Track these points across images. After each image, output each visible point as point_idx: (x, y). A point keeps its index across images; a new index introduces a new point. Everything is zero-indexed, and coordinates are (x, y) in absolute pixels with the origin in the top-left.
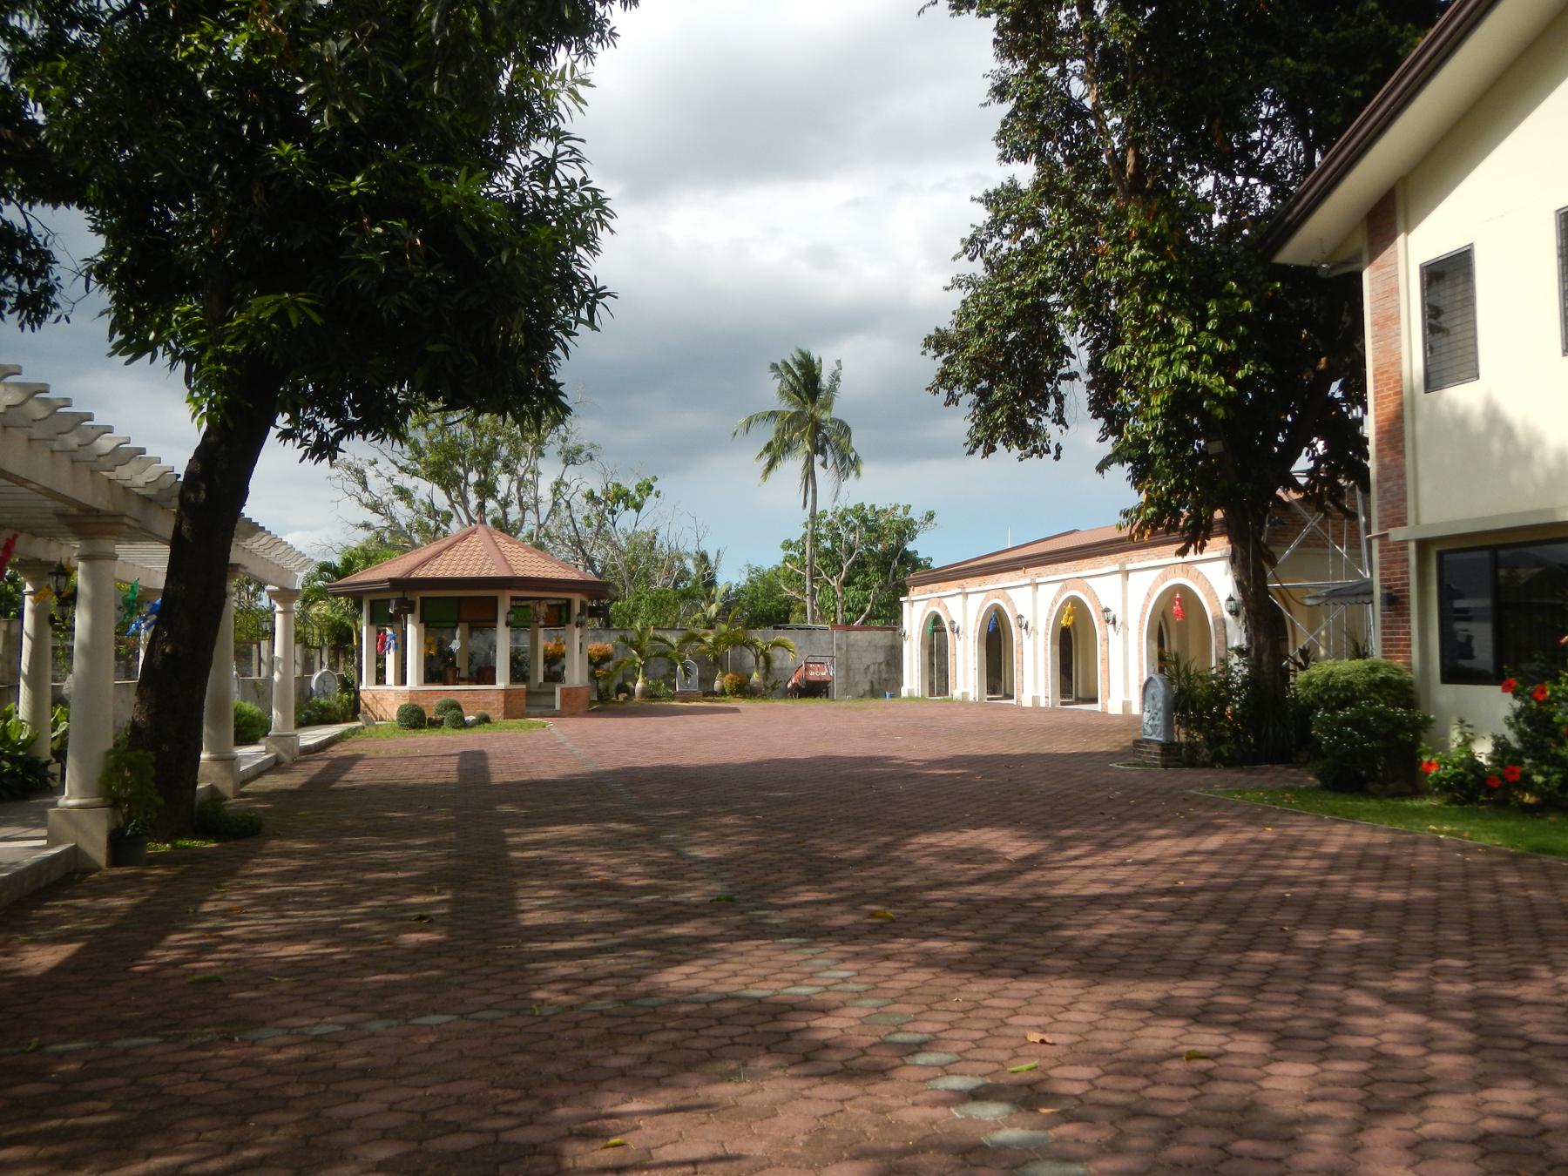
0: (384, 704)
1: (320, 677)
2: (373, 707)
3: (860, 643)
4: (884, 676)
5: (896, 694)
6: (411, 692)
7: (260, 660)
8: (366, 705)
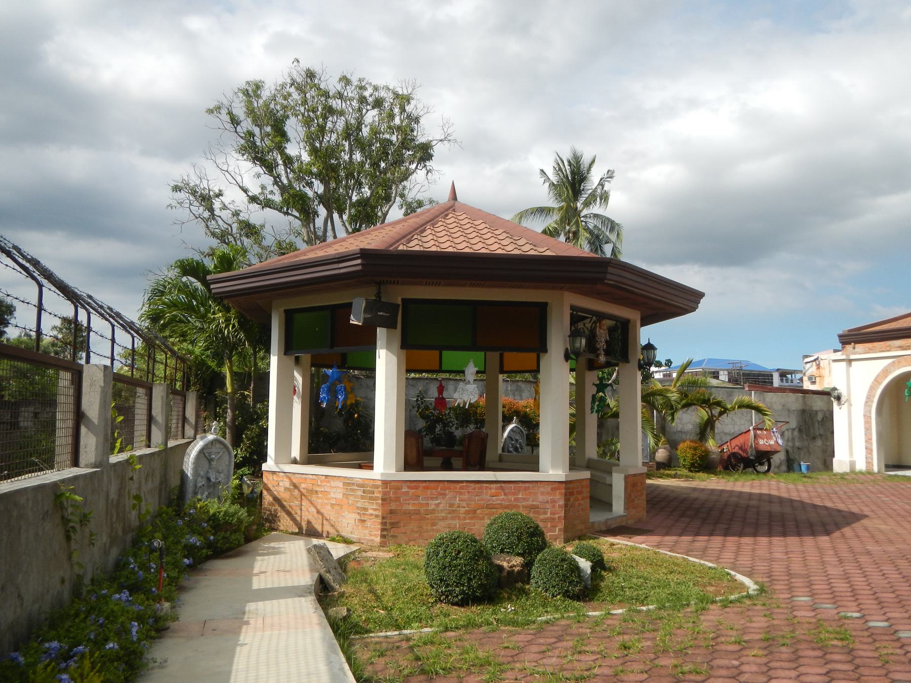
0: (319, 501)
1: (202, 452)
2: (293, 505)
3: (775, 407)
4: (797, 444)
6: (385, 483)
7: (79, 417)
8: (277, 500)
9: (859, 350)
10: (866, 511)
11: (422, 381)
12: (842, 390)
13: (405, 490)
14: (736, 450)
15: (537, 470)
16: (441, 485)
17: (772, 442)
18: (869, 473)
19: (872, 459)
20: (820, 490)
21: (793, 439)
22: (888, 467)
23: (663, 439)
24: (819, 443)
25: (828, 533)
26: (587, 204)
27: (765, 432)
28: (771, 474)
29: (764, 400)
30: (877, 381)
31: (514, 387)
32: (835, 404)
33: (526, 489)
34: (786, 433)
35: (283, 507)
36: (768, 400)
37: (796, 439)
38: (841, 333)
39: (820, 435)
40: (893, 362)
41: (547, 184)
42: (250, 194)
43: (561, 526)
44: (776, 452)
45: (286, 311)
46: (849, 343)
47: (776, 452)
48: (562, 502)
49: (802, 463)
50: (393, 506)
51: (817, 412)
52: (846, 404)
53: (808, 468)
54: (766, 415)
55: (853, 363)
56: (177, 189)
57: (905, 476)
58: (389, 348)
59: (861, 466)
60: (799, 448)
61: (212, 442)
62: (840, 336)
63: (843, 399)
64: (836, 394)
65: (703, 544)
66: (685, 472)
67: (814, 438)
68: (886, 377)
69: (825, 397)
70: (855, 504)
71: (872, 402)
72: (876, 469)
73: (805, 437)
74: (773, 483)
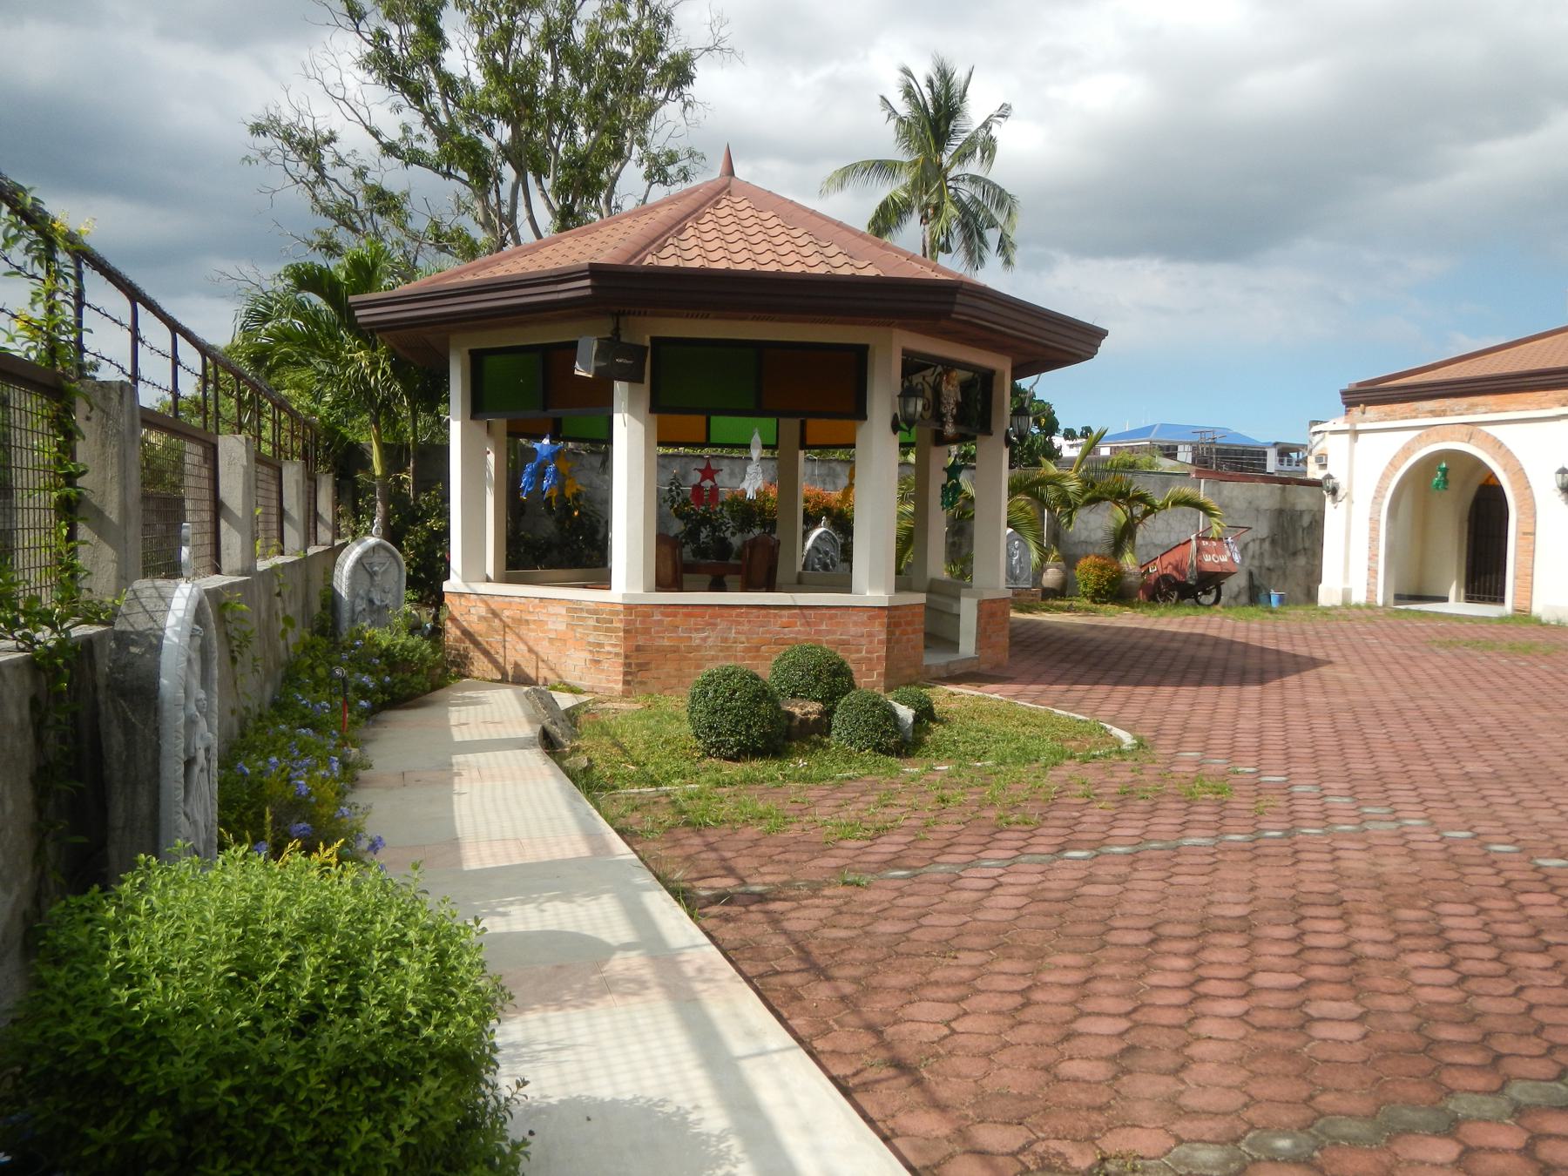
0: (531, 635)
1: (360, 562)
2: (493, 641)
3: (1237, 504)
4: (1268, 563)
5: (1311, 596)
6: (629, 608)
7: (218, 507)
8: (466, 633)
9: (1372, 416)
10: (1335, 655)
11: (678, 460)
12: (1340, 478)
13: (657, 617)
14: (1168, 571)
15: (850, 592)
16: (710, 611)
17: (1224, 559)
18: (1370, 606)
19: (1376, 585)
20: (1282, 629)
21: (1262, 554)
22: (1400, 598)
23: (1055, 553)
24: (1302, 561)
25: (1261, 681)
26: (962, 156)
27: (1214, 544)
28: (1218, 607)
29: (1220, 493)
30: (1393, 465)
31: (824, 470)
32: (1328, 500)
33: (831, 617)
34: (1251, 545)
35: (476, 644)
36: (1225, 492)
37: (1266, 556)
38: (1346, 387)
39: (1305, 549)
40: (1420, 435)
41: (893, 122)
42: (384, 140)
43: (881, 669)
44: (1228, 574)
45: (471, 352)
46: (1356, 404)
47: (1228, 574)
48: (883, 636)
49: (1272, 592)
50: (641, 641)
51: (1302, 512)
52: (1345, 500)
53: (1281, 600)
54: (1214, 515)
55: (1361, 436)
56: (258, 129)
57: (1419, 611)
58: (631, 410)
59: (1359, 597)
60: (1269, 569)
61: (374, 549)
62: (1344, 393)
63: (1341, 493)
64: (1330, 484)
65: (1080, 694)
66: (1086, 603)
67: (1295, 554)
68: (1407, 458)
69: (1317, 489)
70: (1323, 647)
71: (1383, 497)
72: (1380, 602)
73: (1280, 551)
74: (1217, 619)
